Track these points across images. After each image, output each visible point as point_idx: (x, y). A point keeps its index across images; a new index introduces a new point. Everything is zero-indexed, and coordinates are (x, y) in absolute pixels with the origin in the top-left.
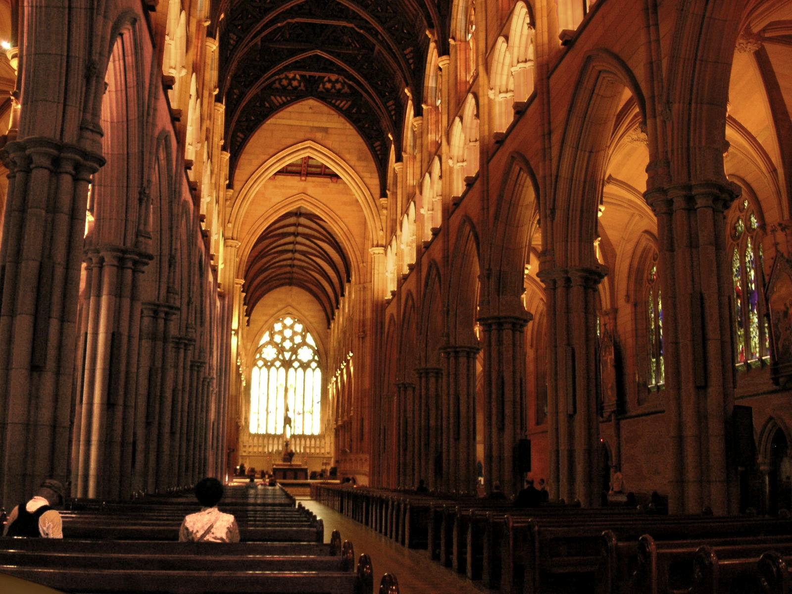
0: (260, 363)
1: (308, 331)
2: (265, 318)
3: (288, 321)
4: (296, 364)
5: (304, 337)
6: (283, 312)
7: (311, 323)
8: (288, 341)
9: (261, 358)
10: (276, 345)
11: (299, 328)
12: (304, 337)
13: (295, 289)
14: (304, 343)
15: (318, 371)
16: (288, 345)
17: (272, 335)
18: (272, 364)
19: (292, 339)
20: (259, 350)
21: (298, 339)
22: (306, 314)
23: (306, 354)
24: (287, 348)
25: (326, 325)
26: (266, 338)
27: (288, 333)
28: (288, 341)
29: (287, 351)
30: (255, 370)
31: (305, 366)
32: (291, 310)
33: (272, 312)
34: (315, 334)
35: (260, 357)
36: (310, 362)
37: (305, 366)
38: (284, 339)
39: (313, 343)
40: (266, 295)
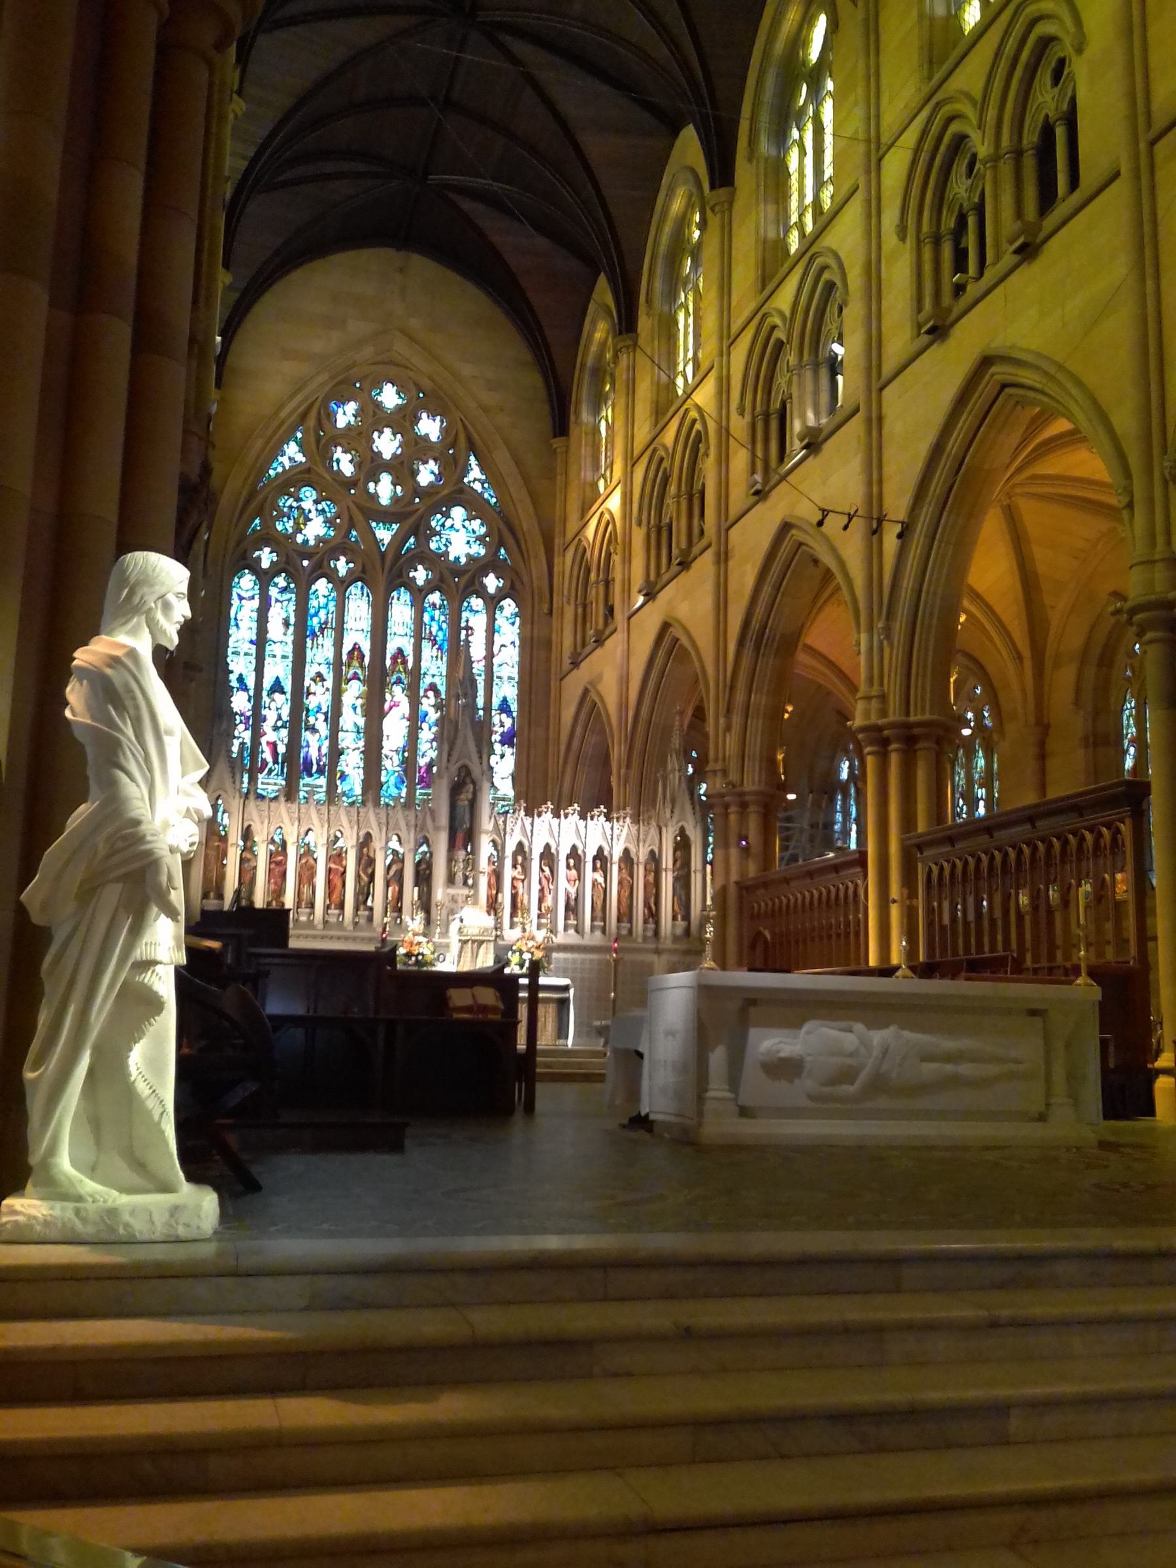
0: (267, 557)
1: (472, 448)
2: (292, 369)
3: (389, 397)
4: (420, 575)
5: (453, 468)
6: (368, 351)
7: (486, 409)
8: (386, 479)
9: (268, 538)
10: (332, 487)
11: (430, 427)
12: (453, 468)
13: (422, 267)
14: (452, 492)
15: (509, 606)
16: (385, 489)
17: (320, 446)
18: (322, 570)
19: (402, 469)
20: (263, 498)
21: (426, 474)
22: (467, 370)
23: (460, 536)
24: (385, 500)
25: (546, 425)
26: (292, 452)
27: (387, 444)
28: (386, 479)
29: (385, 516)
30: (246, 583)
31: (458, 582)
32: (401, 347)
33: (318, 346)
34: (502, 457)
35: (268, 524)
36: (476, 569)
37: (458, 582)
38: (371, 466)
39: (490, 497)
40: (297, 275)
